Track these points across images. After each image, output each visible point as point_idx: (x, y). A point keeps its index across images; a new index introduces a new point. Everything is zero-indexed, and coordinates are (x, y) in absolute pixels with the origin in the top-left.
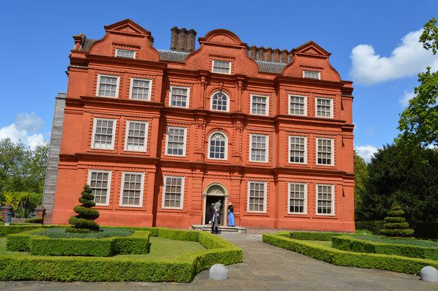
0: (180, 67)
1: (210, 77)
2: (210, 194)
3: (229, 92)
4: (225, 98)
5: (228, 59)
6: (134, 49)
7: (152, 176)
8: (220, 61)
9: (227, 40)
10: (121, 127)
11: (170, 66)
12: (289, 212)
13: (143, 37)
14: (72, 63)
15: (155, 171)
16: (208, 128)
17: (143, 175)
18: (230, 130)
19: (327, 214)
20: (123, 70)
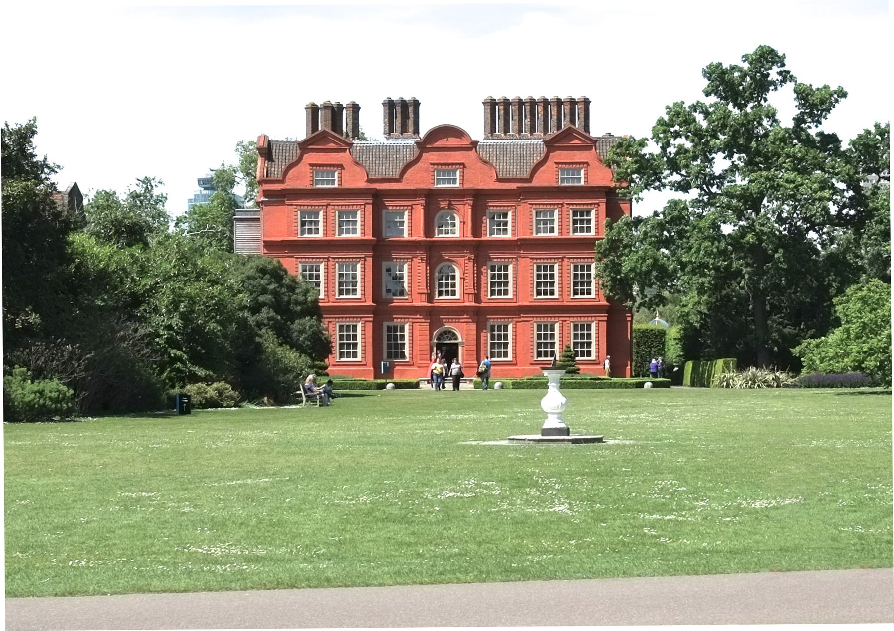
6: (335, 169)
8: (444, 172)
9: (453, 142)
10: (331, 270)
19: (585, 358)
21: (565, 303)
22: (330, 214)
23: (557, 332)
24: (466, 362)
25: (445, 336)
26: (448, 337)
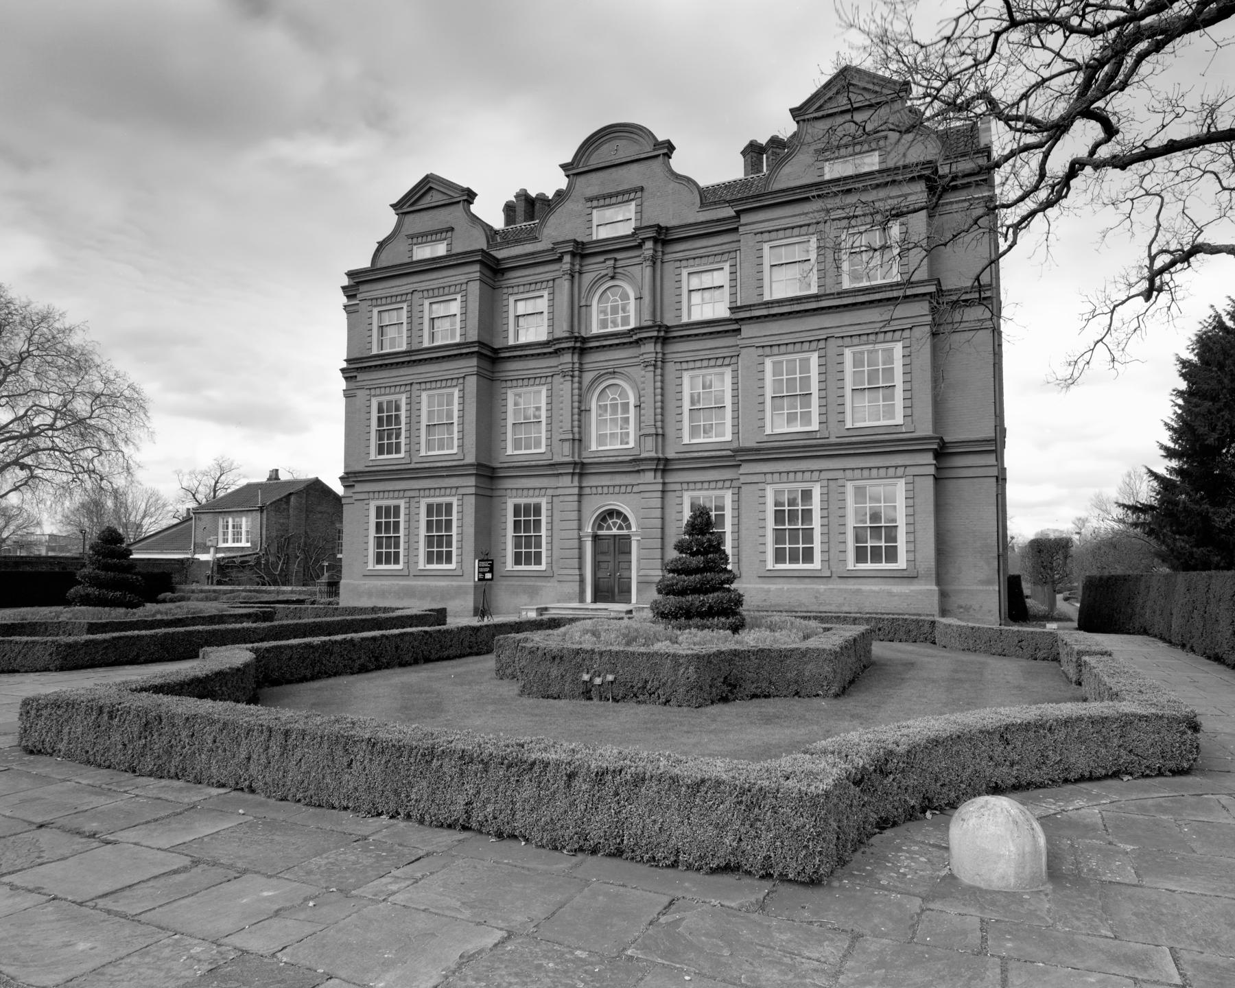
0: (529, 248)
1: (581, 251)
2: (600, 532)
3: (631, 279)
4: (625, 297)
5: (626, 197)
7: (471, 501)
9: (623, 149)
11: (500, 254)
12: (770, 564)
13: (459, 202)
14: (348, 297)
15: (473, 490)
16: (588, 377)
17: (455, 501)
18: (637, 372)
19: (884, 566)
20: (409, 288)
21: (833, 440)
22: (416, 309)
23: (816, 504)
24: (642, 573)
25: (610, 522)
26: (615, 523)
